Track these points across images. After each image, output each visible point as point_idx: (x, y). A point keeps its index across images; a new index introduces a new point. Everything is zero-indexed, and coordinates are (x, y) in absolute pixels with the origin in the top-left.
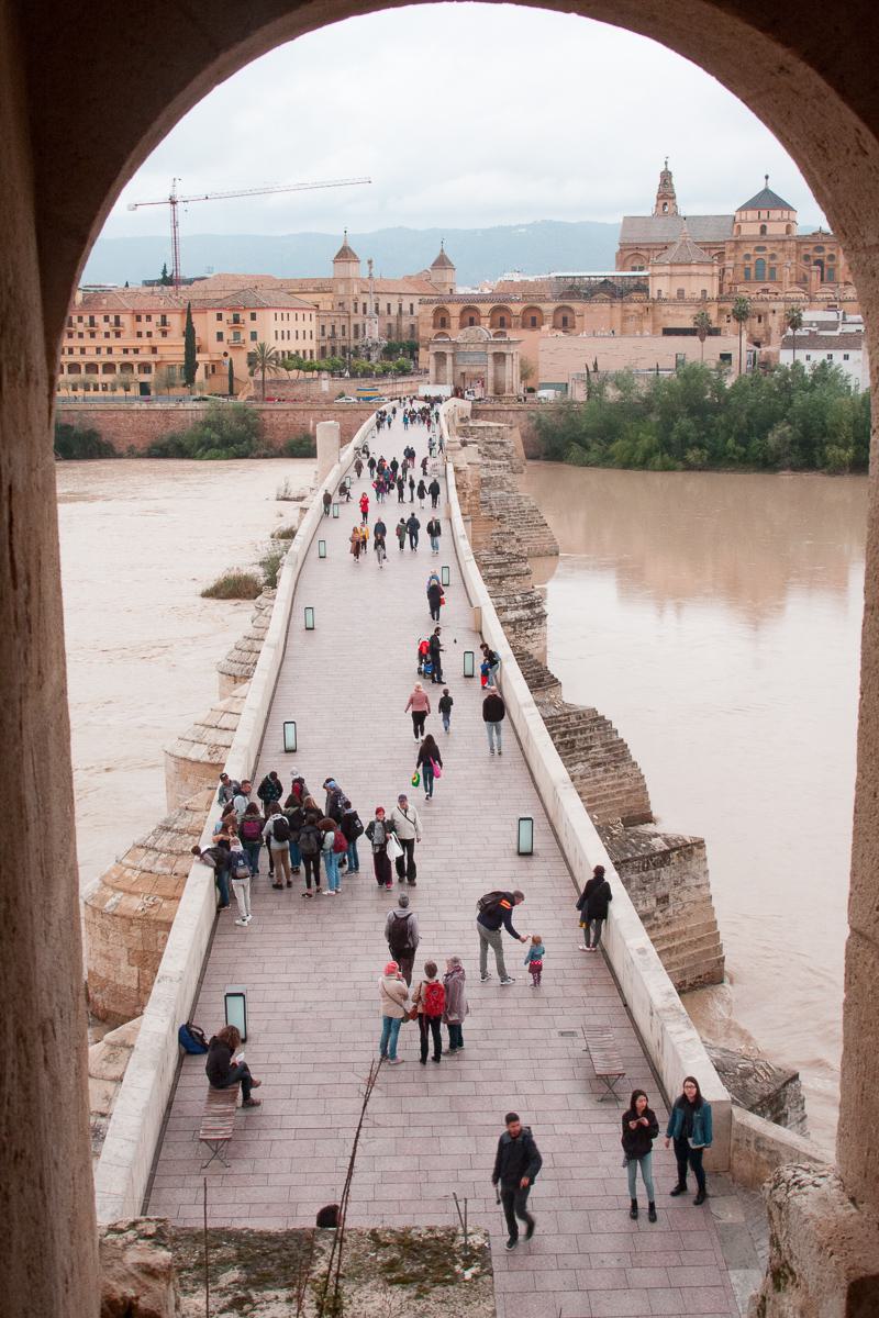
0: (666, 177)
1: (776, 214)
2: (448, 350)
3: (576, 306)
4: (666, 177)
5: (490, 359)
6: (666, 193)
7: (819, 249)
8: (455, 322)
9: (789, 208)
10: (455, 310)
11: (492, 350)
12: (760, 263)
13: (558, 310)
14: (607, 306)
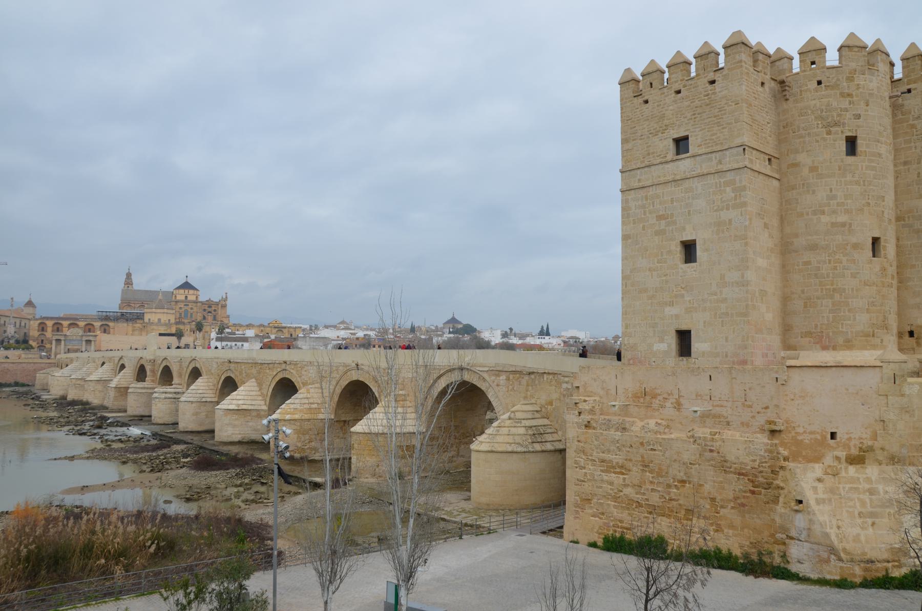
0: (129, 275)
1: (191, 292)
2: (62, 338)
3: (111, 324)
4: (129, 275)
5: (84, 343)
6: (129, 281)
7: (210, 307)
8: (49, 329)
9: (197, 290)
10: (50, 323)
11: (85, 338)
12: (186, 311)
13: (102, 325)
14: (125, 325)
